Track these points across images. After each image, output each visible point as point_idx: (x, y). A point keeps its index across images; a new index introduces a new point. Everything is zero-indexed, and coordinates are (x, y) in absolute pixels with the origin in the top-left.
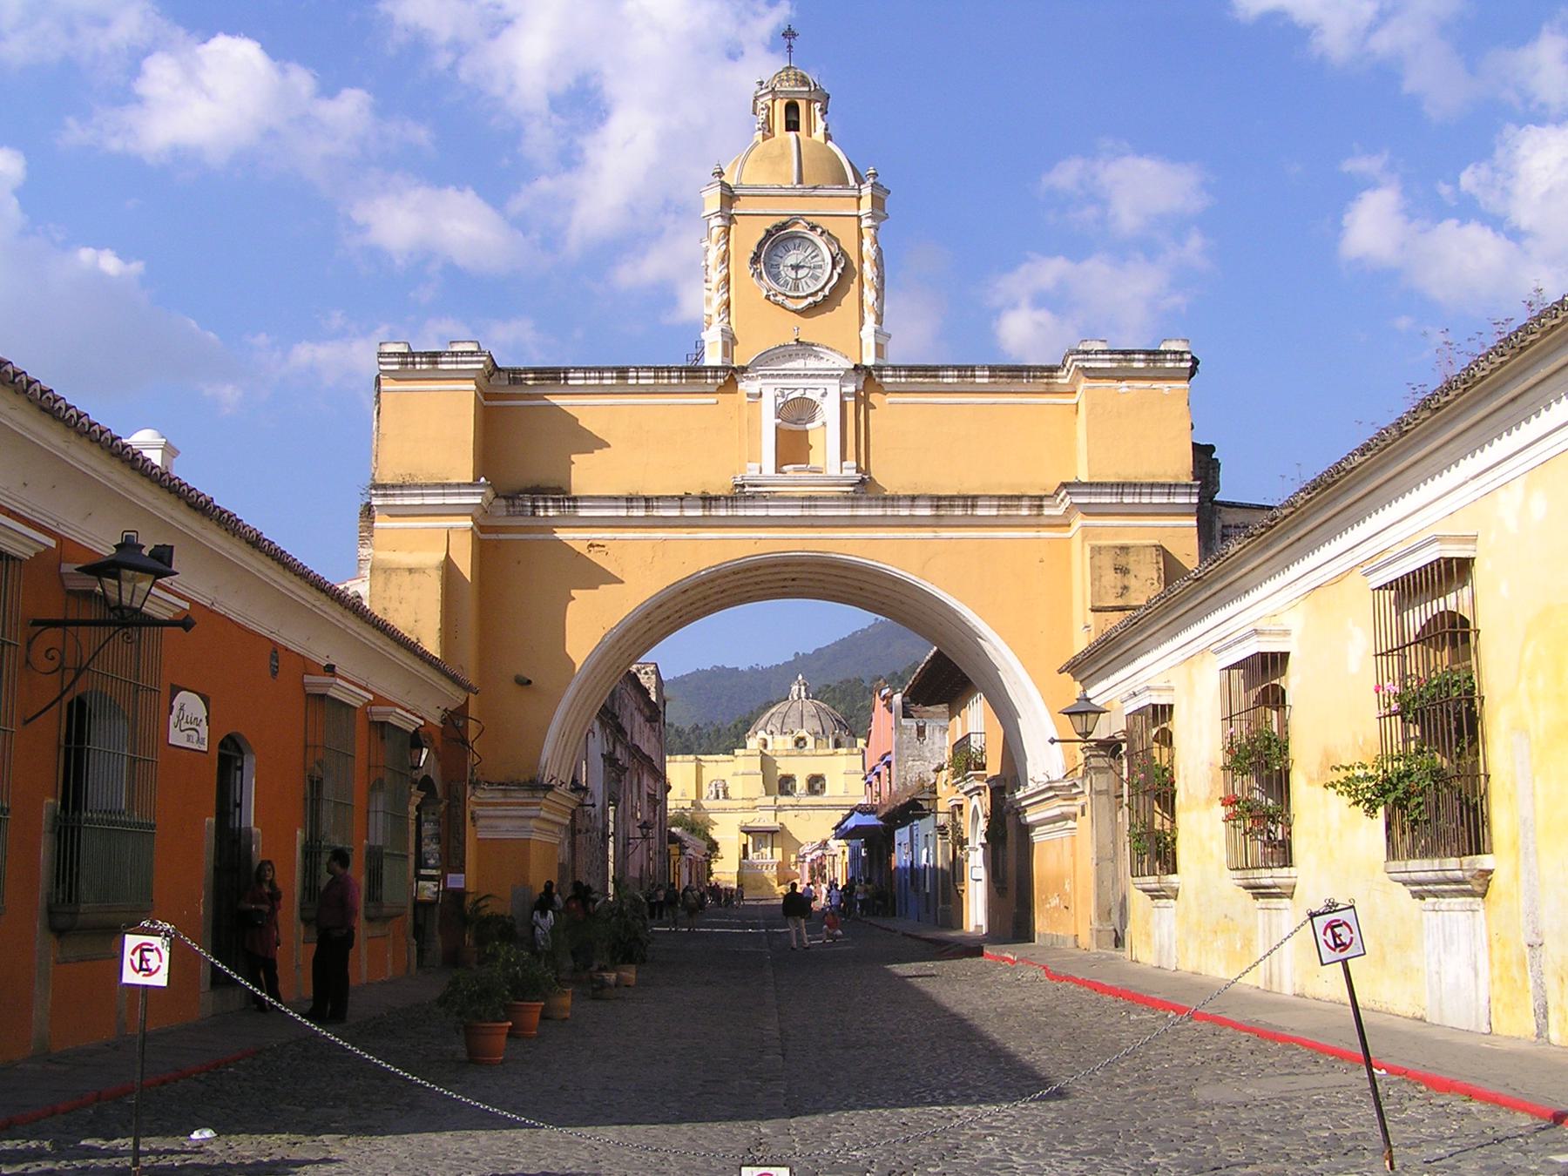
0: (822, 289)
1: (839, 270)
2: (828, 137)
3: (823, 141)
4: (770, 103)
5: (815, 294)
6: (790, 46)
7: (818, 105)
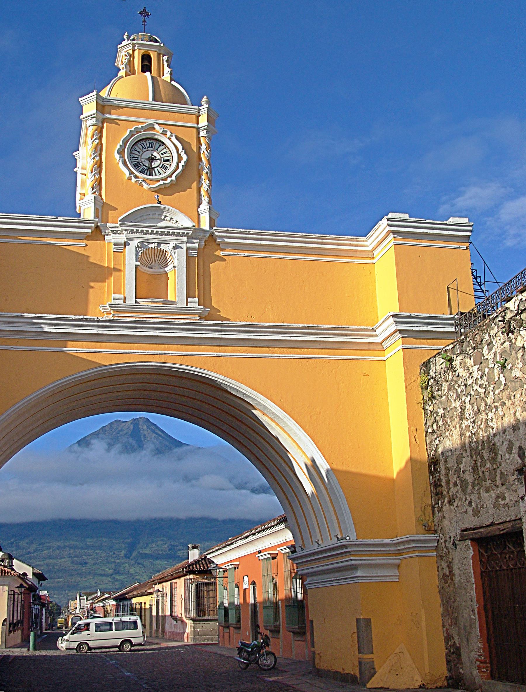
0: (170, 176)
1: (182, 163)
4: (131, 52)
6: (144, 21)
7: (165, 58)
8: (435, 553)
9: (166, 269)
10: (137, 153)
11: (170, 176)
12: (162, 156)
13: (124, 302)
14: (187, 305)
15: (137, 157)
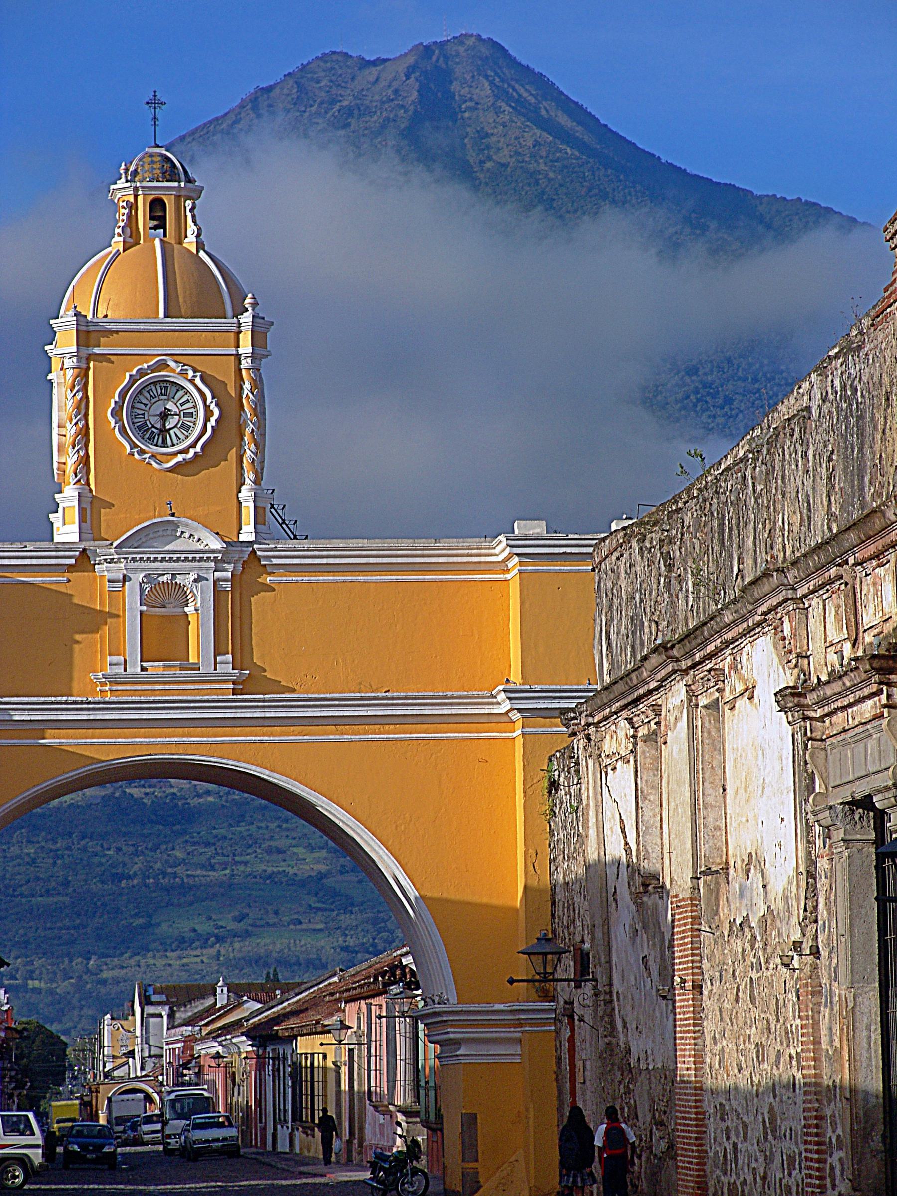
0: (193, 445)
1: (212, 422)
2: (200, 245)
3: (194, 251)
4: (132, 199)
5: (185, 451)
8: (553, 1028)
9: (186, 609)
10: (142, 406)
11: (193, 445)
12: (181, 408)
13: (125, 670)
14: (215, 669)
15: (143, 414)
